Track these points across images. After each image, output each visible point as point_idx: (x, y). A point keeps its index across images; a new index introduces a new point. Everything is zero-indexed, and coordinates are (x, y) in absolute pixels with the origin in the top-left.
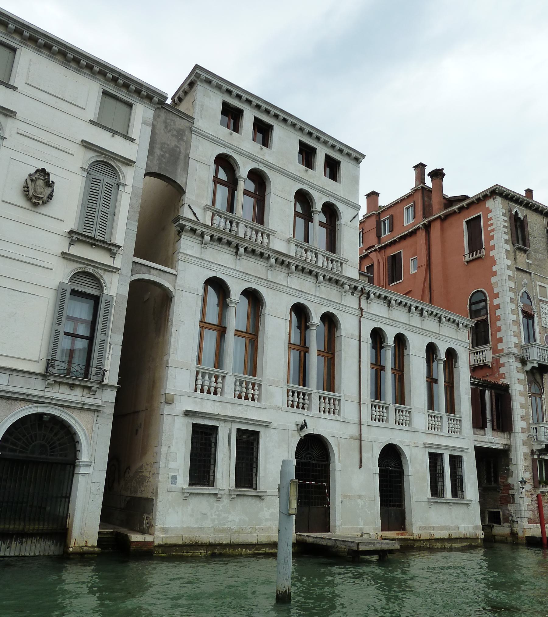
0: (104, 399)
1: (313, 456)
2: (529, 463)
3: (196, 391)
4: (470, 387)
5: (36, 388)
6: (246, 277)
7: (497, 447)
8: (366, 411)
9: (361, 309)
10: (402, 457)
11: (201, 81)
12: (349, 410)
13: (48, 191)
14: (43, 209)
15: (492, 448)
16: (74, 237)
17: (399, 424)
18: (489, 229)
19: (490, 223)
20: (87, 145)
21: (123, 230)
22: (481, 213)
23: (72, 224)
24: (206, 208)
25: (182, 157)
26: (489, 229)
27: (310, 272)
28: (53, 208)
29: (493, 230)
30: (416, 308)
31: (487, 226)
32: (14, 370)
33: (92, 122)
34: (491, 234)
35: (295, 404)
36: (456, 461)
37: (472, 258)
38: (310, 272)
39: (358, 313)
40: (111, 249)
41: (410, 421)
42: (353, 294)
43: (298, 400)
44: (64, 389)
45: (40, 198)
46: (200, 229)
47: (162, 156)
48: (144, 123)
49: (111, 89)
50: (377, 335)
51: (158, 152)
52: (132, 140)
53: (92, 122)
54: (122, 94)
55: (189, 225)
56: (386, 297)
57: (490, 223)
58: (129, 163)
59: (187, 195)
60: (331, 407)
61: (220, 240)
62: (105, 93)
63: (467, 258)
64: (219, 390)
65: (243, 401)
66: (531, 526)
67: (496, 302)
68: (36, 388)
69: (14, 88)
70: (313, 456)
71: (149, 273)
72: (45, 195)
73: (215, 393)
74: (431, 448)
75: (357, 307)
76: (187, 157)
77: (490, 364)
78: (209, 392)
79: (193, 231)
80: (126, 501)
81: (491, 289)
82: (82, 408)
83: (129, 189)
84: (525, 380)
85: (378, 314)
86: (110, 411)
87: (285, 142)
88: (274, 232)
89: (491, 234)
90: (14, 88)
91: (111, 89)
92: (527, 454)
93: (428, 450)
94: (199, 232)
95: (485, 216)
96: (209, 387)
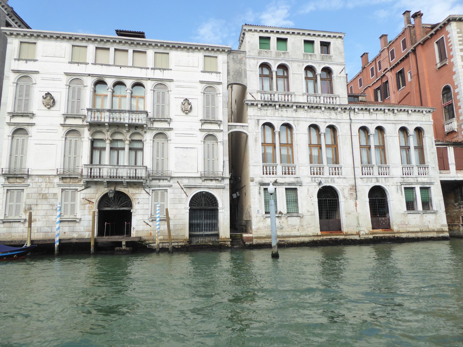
0: (225, 183)
3: (264, 174)
4: (435, 147)
5: (199, 182)
6: (282, 119)
8: (358, 171)
9: (351, 119)
10: (386, 191)
11: (247, 32)
13: (190, 106)
14: (190, 114)
17: (382, 174)
18: (449, 45)
19: (449, 41)
20: (202, 82)
21: (222, 113)
22: (444, 36)
23: (201, 117)
24: (258, 92)
25: (243, 72)
26: (449, 45)
27: (317, 107)
29: (451, 45)
30: (389, 110)
31: (448, 43)
32: (190, 177)
34: (451, 48)
36: (425, 190)
37: (442, 65)
38: (317, 107)
39: (349, 121)
40: (218, 123)
41: (389, 172)
42: (345, 112)
44: (210, 182)
45: (187, 110)
46: (255, 103)
47: (234, 75)
48: (223, 63)
51: (231, 73)
52: (220, 73)
54: (212, 54)
55: (250, 103)
56: (366, 109)
57: (449, 41)
58: (219, 83)
59: (248, 89)
60: (337, 171)
61: (266, 105)
62: (205, 56)
63: (439, 65)
64: (274, 172)
65: (287, 175)
67: (456, 91)
68: (199, 182)
69: (171, 70)
71: (236, 128)
72: (189, 109)
73: (273, 174)
74: (405, 185)
75: (348, 118)
76: (245, 71)
77: (456, 130)
78: (270, 174)
79: (252, 104)
80: (239, 221)
81: (453, 83)
82: (217, 188)
83: (221, 95)
85: (363, 118)
86: (228, 187)
87: (295, 43)
88: (294, 93)
89: (451, 48)
90: (171, 70)
91: (207, 54)
93: (403, 187)
94: (255, 104)
95: (446, 36)
96: (270, 172)
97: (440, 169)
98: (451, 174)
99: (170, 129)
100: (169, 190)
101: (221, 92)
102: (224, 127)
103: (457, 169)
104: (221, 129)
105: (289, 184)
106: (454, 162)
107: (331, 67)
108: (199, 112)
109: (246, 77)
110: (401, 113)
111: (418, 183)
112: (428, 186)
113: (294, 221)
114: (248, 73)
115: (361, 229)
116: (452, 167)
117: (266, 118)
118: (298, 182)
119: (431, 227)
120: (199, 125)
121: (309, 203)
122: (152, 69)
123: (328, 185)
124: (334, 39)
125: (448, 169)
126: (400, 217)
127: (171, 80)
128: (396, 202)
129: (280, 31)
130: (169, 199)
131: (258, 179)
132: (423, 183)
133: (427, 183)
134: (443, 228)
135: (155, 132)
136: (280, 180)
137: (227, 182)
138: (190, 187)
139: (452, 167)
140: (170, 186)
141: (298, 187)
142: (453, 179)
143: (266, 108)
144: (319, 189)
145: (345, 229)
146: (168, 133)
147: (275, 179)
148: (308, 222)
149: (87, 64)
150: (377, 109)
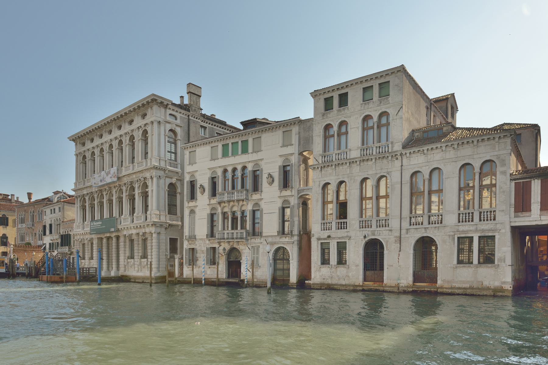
20: (280, 156)
33: (281, 147)
42: (397, 159)
49: (285, 129)
52: (293, 145)
53: (281, 147)
54: (288, 128)
82: (288, 243)
86: (296, 243)
91: (285, 129)
97: (516, 211)
98: (532, 216)
99: (261, 199)
100: (261, 246)
104: (293, 194)
105: (339, 238)
106: (539, 200)
107: (388, 110)
109: (312, 143)
110: (466, 146)
111: (476, 231)
112: (490, 234)
113: (342, 270)
114: (314, 138)
115: (402, 281)
116: (536, 206)
117: (325, 179)
118: (347, 236)
119: (486, 283)
120: (278, 193)
121: (355, 255)
122: (251, 153)
123: (373, 237)
124: (393, 75)
126: (449, 271)
127: (262, 160)
129: (340, 87)
131: (316, 236)
132: (483, 231)
133: (489, 230)
134: (503, 286)
135: (253, 203)
137: (296, 238)
138: (272, 244)
139: (536, 206)
141: (347, 241)
142: (534, 223)
143: (326, 169)
144: (364, 242)
145: (385, 281)
147: (329, 234)
149: (218, 159)
150: (432, 149)
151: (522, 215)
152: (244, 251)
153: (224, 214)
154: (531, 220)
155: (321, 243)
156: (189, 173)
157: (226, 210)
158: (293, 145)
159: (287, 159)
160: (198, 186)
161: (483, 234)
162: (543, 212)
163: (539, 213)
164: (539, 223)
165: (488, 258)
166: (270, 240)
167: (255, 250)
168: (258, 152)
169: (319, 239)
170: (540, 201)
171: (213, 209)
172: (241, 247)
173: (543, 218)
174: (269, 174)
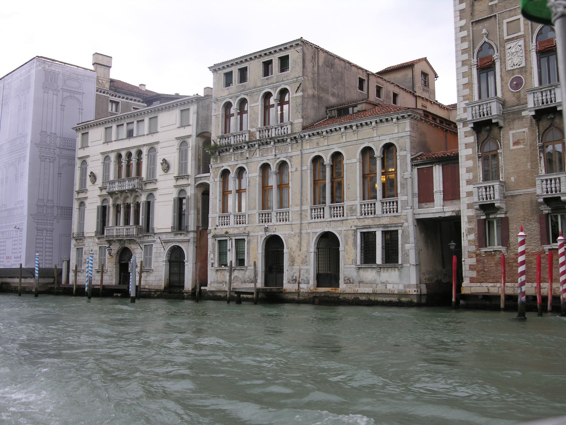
1: (274, 246)
2: (474, 225)
7: (447, 215)
12: (294, 217)
15: (440, 217)
16: (177, 178)
17: (334, 216)
23: (176, 174)
28: (171, 171)
33: (178, 128)
35: (264, 220)
43: (265, 218)
44: (179, 236)
48: (194, 114)
49: (183, 108)
50: (317, 160)
52: (190, 125)
53: (178, 128)
58: (189, 136)
66: (473, 284)
68: (171, 237)
70: (274, 246)
74: (362, 229)
82: (183, 241)
84: (475, 142)
86: (192, 240)
92: (472, 216)
97: (420, 202)
101: (191, 145)
102: (191, 181)
103: (445, 199)
104: (189, 183)
108: (174, 170)
116: (438, 197)
120: (173, 182)
125: (433, 201)
128: (349, 253)
130: (153, 253)
135: (147, 193)
136: (231, 231)
138: (167, 242)
139: (438, 197)
140: (154, 241)
141: (246, 238)
142: (437, 216)
146: (155, 193)
148: (251, 277)
151: (426, 206)
152: (136, 251)
153: (117, 208)
154: (434, 211)
155: (219, 241)
156: (80, 158)
157: (120, 202)
158: (190, 125)
159: (184, 141)
160: (88, 173)
161: (386, 229)
162: (446, 202)
163: (442, 204)
164: (442, 215)
165: (391, 256)
166: (164, 237)
167: (148, 249)
168: (154, 133)
169: (214, 237)
170: (442, 189)
171: (104, 200)
172: (132, 247)
173: (446, 209)
174: (164, 160)
